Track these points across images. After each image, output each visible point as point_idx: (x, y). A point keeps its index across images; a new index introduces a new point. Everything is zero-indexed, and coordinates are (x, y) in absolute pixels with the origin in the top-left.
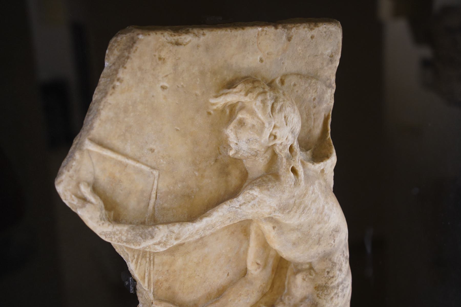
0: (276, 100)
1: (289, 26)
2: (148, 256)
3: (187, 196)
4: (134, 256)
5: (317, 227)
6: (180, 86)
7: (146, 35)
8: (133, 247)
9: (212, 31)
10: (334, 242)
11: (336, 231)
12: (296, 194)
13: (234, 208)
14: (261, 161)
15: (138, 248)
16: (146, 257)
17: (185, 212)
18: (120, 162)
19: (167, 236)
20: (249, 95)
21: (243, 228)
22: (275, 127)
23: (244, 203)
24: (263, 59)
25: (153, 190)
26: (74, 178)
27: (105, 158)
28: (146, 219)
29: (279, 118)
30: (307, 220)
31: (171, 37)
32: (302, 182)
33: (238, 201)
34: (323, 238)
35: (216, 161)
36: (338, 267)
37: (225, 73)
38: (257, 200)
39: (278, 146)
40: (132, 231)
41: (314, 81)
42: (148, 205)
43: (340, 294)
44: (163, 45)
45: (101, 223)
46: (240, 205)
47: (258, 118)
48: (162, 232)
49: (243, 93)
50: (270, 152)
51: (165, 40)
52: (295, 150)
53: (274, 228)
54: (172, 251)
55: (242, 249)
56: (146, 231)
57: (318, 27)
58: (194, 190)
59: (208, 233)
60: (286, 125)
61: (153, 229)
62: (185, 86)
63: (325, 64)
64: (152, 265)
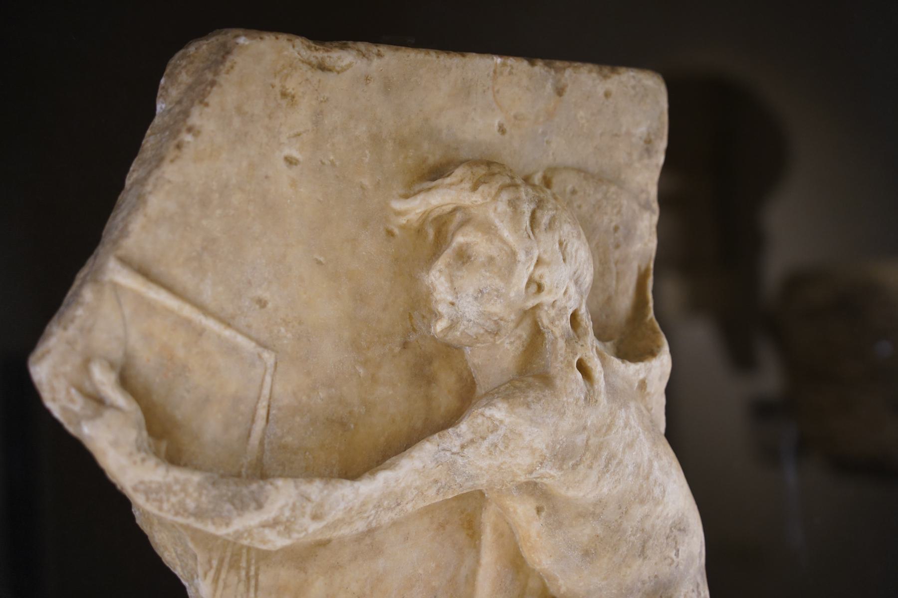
0: (540, 204)
1: (558, 64)
2: (244, 564)
3: (339, 423)
4: (209, 562)
5: (638, 512)
6: (327, 162)
7: (254, 38)
8: (211, 528)
9: (397, 50)
10: (677, 555)
11: (680, 530)
12: (589, 424)
13: (448, 454)
14: (507, 346)
15: (222, 531)
16: (239, 568)
17: (334, 462)
18: (187, 323)
19: (293, 508)
20: (481, 188)
22: (539, 262)
23: (472, 441)
24: (507, 127)
25: (262, 398)
26: (79, 347)
27: (151, 308)
28: (243, 470)
29: (547, 244)
30: (615, 492)
31: (309, 52)
32: (603, 396)
33: (459, 436)
34: (651, 542)
35: (405, 345)
37: (426, 146)
38: (501, 432)
39: (546, 308)
40: (210, 487)
41: (613, 189)
42: (249, 435)
45: (138, 457)
46: (463, 447)
47: (503, 241)
48: (282, 495)
49: (467, 185)
50: (527, 323)
51: (296, 54)
52: (583, 324)
53: (539, 510)
54: (303, 556)
55: (464, 571)
56: (245, 491)
57: (619, 74)
58: (356, 409)
59: (386, 518)
60: (564, 260)
61: (261, 487)
62: (337, 163)
64: (252, 590)
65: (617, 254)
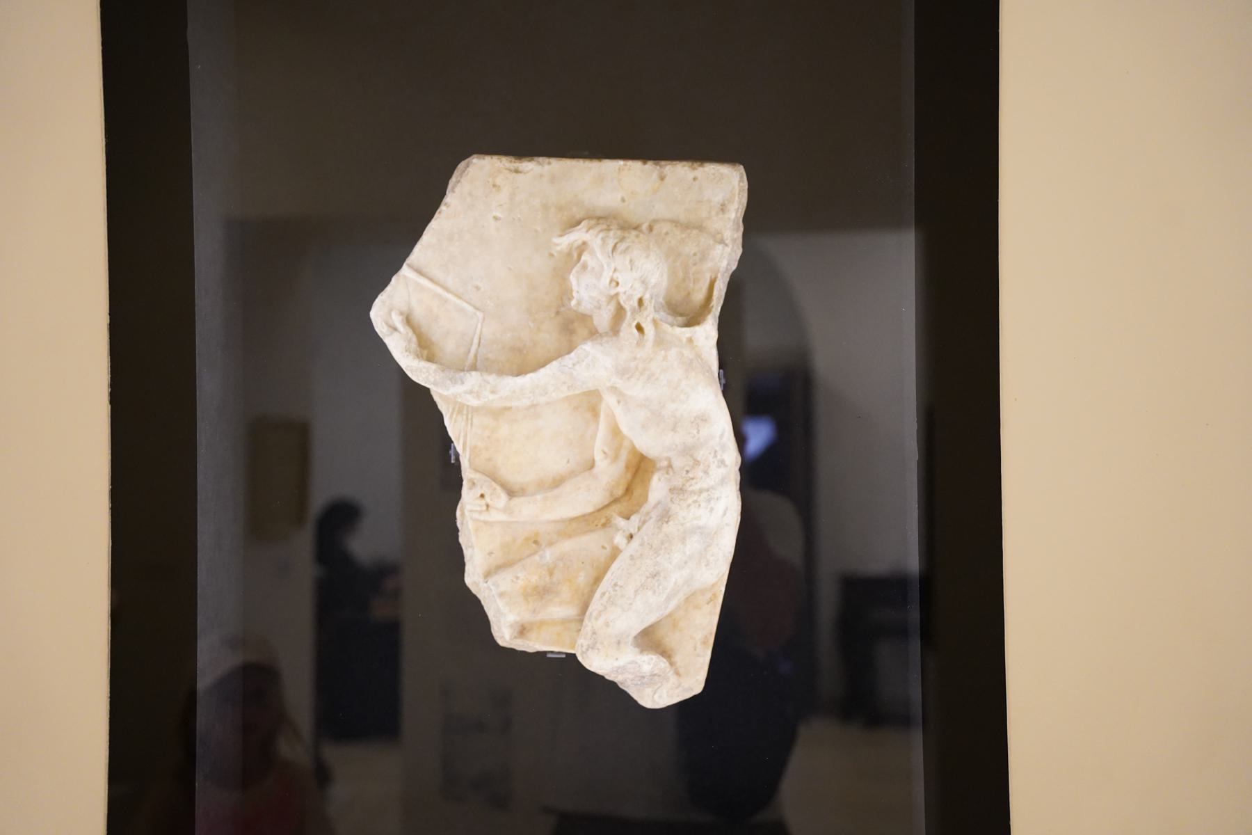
0: (622, 239)
1: (663, 163)
8: (440, 391)
15: (445, 393)
21: (590, 403)
22: (615, 270)
29: (621, 261)
35: (558, 313)
36: (702, 467)
37: (574, 209)
41: (695, 232)
43: (703, 504)
44: (499, 171)
48: (473, 379)
50: (613, 303)
53: (619, 402)
63: (713, 213)
65: (694, 269)
